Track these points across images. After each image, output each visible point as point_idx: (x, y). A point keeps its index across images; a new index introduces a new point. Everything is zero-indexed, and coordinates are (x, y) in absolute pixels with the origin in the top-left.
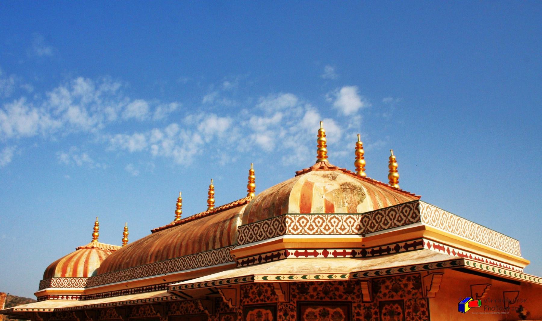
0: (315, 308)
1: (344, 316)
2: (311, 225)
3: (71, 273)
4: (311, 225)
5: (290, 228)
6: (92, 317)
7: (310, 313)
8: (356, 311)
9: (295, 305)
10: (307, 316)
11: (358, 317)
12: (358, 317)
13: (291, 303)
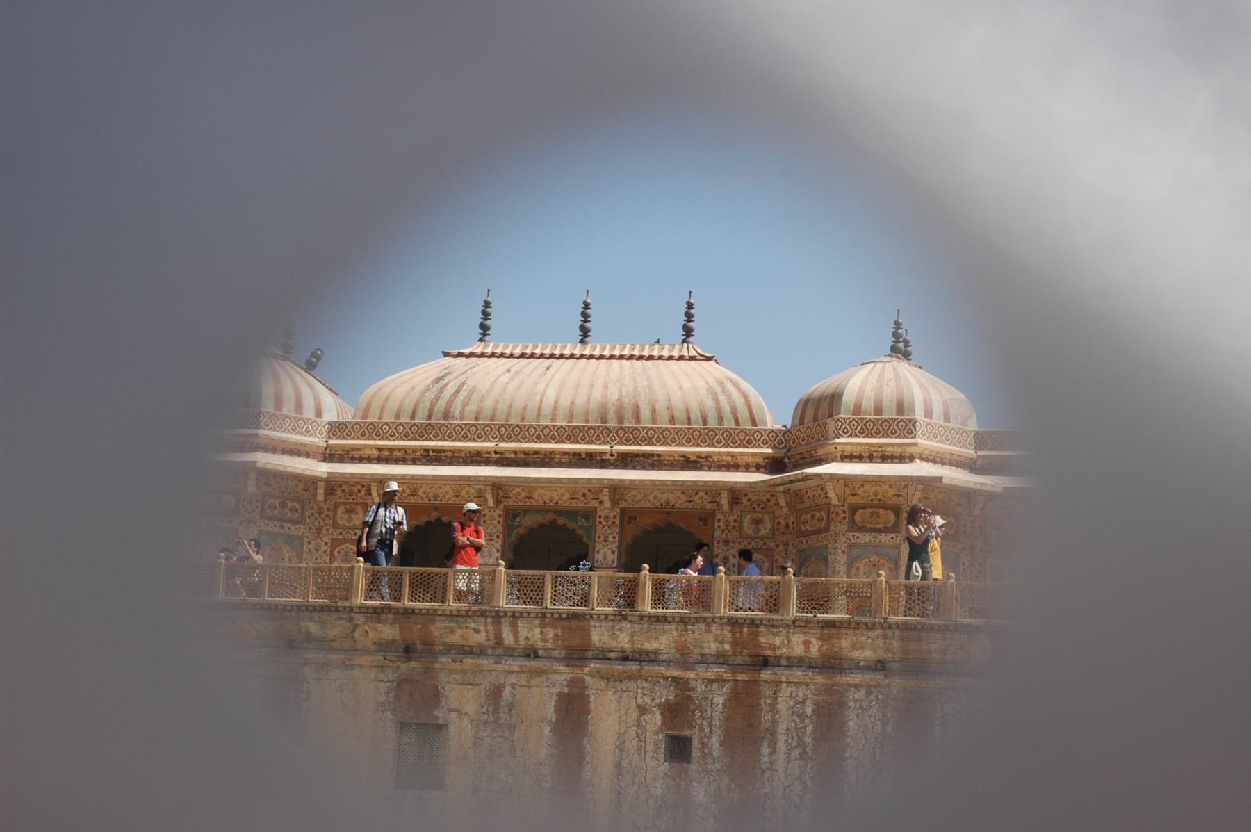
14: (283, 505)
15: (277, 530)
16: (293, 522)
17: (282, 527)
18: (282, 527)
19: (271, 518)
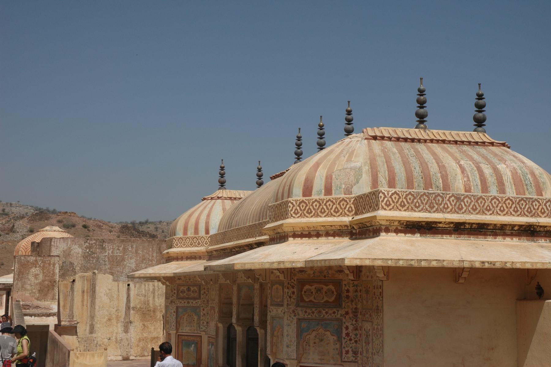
0: (312, 286)
1: (335, 293)
2: (309, 208)
3: (193, 231)
4: (309, 208)
5: (292, 212)
6: (211, 280)
7: (307, 289)
8: (346, 289)
9: (295, 283)
10: (305, 292)
11: (347, 294)
12: (347, 294)
13: (292, 281)
14: (189, 290)
15: (186, 305)
16: (195, 299)
17: (188, 303)
18: (188, 303)
19: (182, 298)
